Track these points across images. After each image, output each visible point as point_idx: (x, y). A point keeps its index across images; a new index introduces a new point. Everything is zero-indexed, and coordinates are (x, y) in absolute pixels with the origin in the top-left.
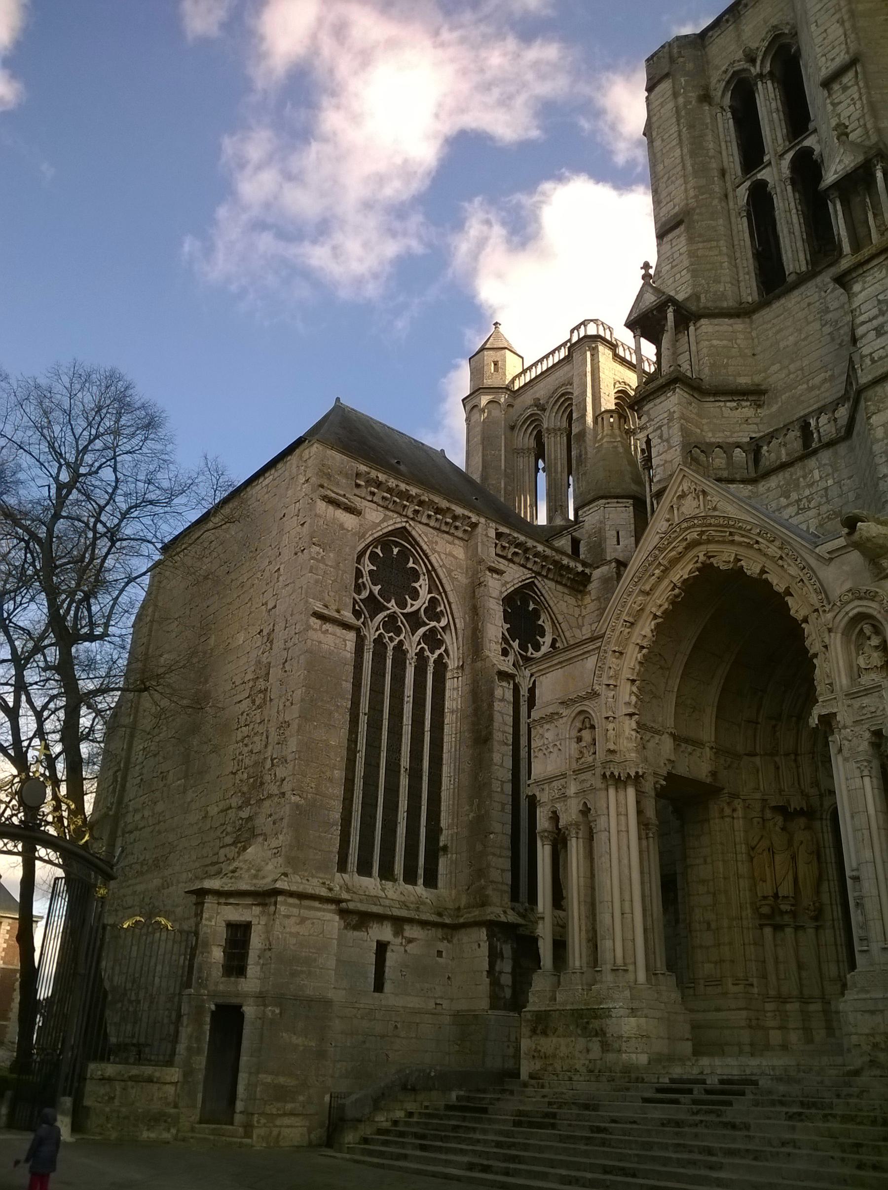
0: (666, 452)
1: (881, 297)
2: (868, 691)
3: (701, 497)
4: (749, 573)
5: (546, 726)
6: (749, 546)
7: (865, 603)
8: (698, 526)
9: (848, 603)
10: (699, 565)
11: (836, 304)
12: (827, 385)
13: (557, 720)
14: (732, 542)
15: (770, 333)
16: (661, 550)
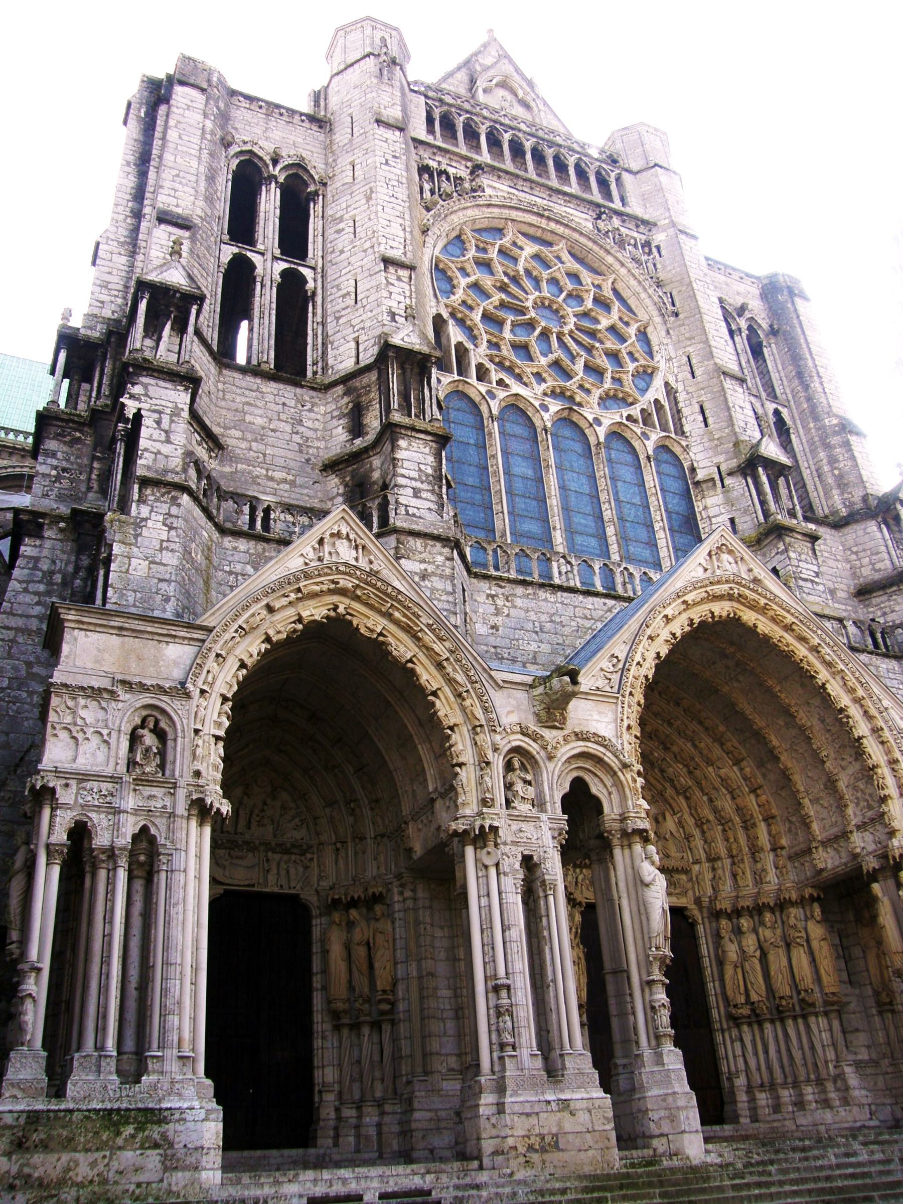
0: (162, 442)
1: (423, 467)
2: (526, 819)
3: (360, 551)
4: (395, 653)
5: (82, 702)
6: (407, 629)
7: (527, 739)
8: (358, 579)
9: (513, 733)
10: (332, 614)
11: (309, 424)
12: (287, 487)
13: (107, 700)
14: (388, 616)
15: (238, 399)
16: (307, 576)
